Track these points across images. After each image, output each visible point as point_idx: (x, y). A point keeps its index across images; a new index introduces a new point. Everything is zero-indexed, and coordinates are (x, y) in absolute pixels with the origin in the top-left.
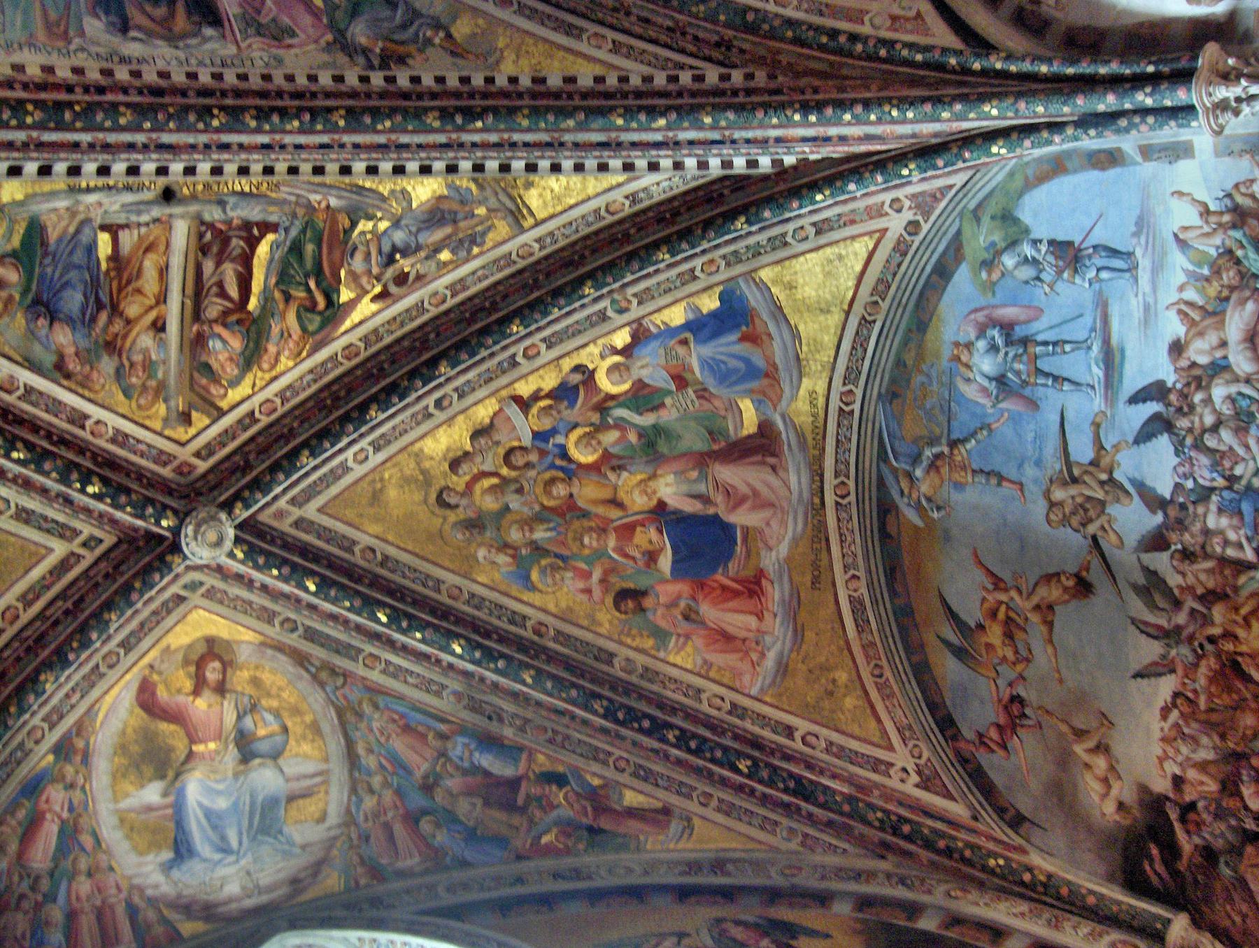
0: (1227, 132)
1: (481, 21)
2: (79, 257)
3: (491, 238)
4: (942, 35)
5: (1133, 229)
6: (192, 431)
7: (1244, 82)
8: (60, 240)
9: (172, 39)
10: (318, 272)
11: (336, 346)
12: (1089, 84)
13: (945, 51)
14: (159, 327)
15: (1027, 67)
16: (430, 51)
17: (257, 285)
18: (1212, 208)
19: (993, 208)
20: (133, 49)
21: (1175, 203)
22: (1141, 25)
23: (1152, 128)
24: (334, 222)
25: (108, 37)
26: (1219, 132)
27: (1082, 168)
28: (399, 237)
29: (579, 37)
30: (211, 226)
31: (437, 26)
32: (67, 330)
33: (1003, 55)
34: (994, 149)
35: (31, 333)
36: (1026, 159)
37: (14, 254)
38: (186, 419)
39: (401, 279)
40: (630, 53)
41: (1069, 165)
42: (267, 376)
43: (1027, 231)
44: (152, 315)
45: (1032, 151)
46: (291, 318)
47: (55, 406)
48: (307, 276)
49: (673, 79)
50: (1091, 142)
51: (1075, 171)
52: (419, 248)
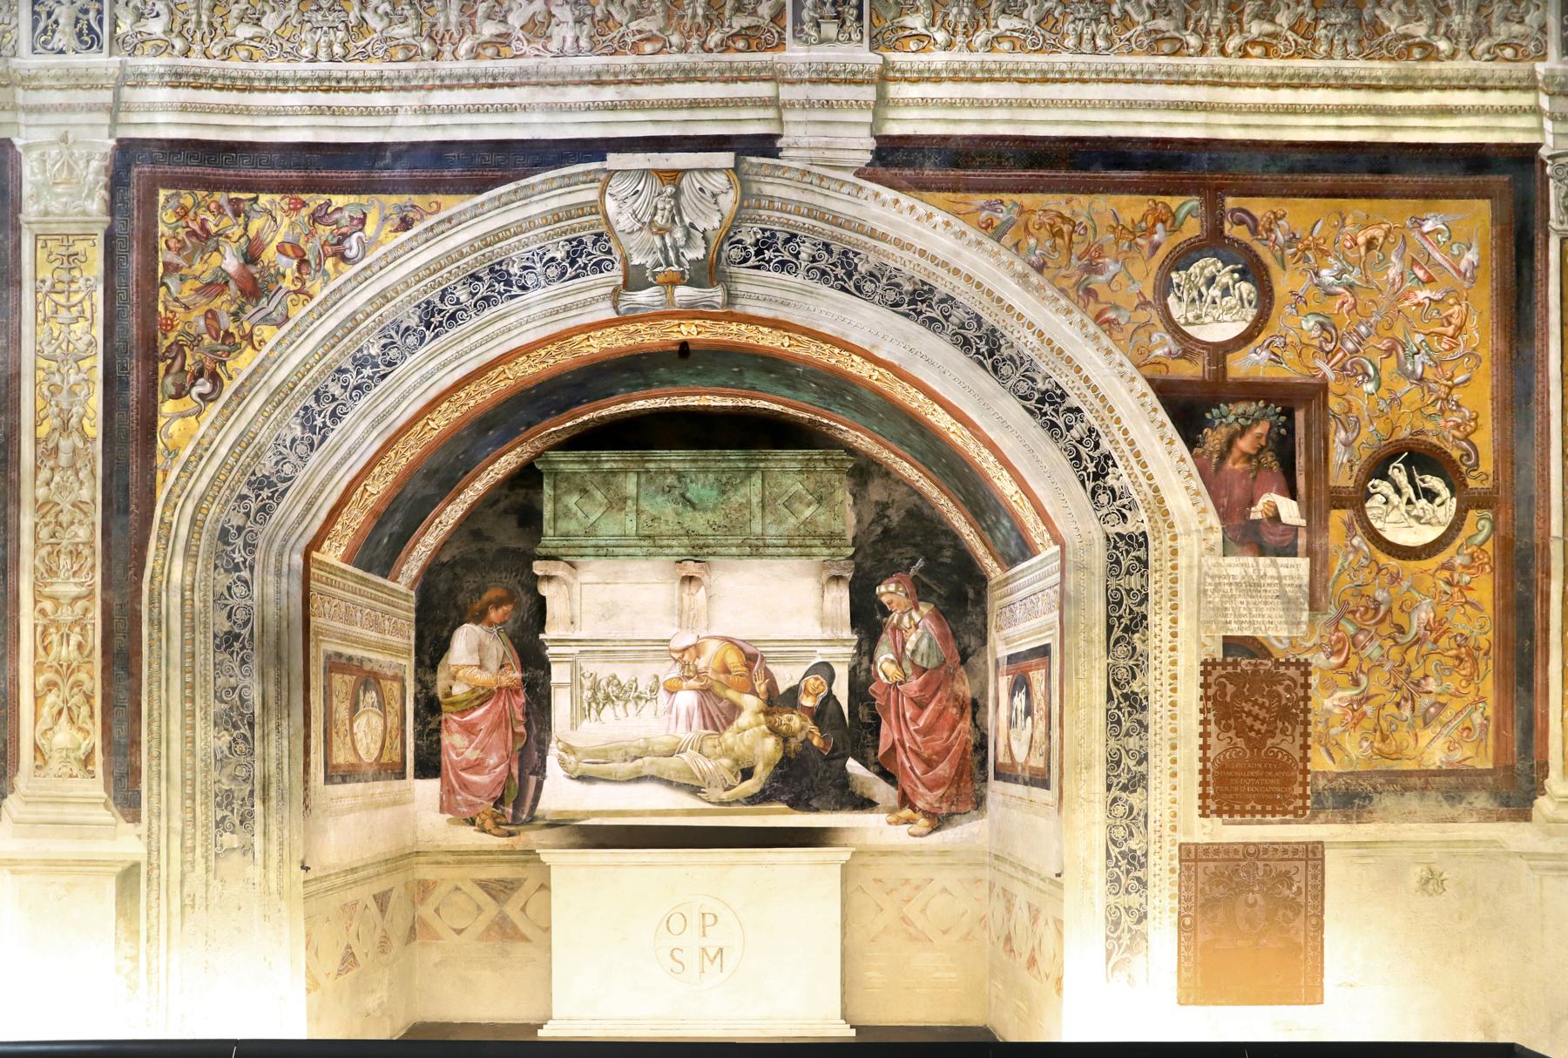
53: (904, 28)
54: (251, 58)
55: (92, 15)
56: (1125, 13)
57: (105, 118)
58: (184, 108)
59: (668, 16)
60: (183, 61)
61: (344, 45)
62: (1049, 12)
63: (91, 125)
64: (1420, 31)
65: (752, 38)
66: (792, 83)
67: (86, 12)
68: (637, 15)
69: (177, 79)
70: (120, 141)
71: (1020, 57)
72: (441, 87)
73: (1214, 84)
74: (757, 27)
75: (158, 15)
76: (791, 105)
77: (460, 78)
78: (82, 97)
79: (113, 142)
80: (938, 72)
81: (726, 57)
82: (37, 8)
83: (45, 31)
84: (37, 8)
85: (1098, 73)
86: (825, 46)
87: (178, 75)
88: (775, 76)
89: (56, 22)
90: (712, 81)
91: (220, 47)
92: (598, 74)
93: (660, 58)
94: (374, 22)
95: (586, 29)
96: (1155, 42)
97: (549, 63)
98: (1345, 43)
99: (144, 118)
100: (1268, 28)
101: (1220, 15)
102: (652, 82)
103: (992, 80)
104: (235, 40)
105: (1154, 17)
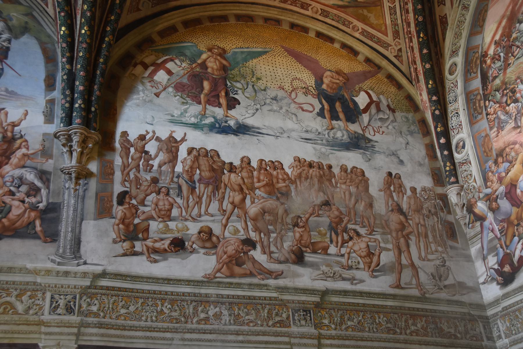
0: (55, 140)
4: (126, 19)
5: (10, 89)
7: (79, 150)
12: (90, 81)
13: (119, 16)
15: (104, 52)
18: (16, 128)
19: (32, 24)
21: (21, 111)
22: (116, 110)
23: (62, 105)
26: (56, 136)
27: (47, 71)
33: (112, 42)
34: (63, 28)
36: (56, 45)
41: (50, 65)
43: (16, 37)
45: (59, 48)
50: (60, 76)
51: (46, 67)
53: (323, 323)
54: (125, 319)
55: (72, 303)
56: (380, 322)
57: (74, 338)
58: (102, 335)
59: (257, 316)
60: (103, 320)
61: (156, 317)
62: (360, 321)
63: (69, 340)
64: (452, 331)
65: (281, 323)
66: (294, 338)
67: (70, 302)
68: (247, 314)
69: (100, 326)
70: (79, 346)
71: (355, 333)
72: (188, 332)
73: (405, 343)
74: (283, 321)
75: (95, 305)
76: (294, 344)
77: (194, 330)
78: (66, 330)
79: (76, 346)
80: (334, 336)
81: (275, 329)
82: (53, 300)
83: (55, 307)
84: (53, 300)
85: (376, 338)
86: (302, 327)
87: (101, 324)
88: (289, 335)
89: (59, 305)
90: (271, 336)
91: (115, 316)
92: (237, 331)
93: (255, 328)
94: (165, 310)
95: (232, 317)
96: (389, 331)
97: (221, 327)
98: (435, 333)
99: (85, 338)
100: (416, 328)
101: (403, 324)
102: (253, 335)
103: (348, 339)
104: (120, 313)
105: (387, 323)
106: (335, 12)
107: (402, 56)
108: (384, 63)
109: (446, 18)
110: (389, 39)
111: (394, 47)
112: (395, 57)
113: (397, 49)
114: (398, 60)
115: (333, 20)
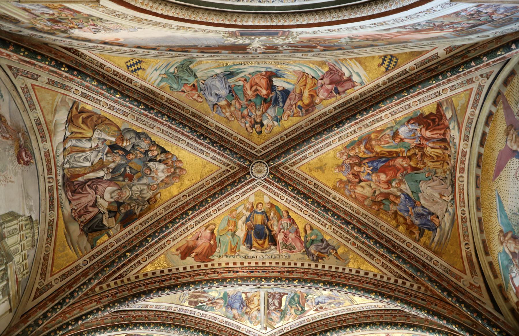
1: (346, 249)
2: (237, 297)
3: (345, 304)
6: (267, 331)
8: (232, 295)
9: (262, 250)
10: (299, 303)
11: (305, 318)
14: (259, 310)
16: (330, 256)
17: (283, 304)
20: (252, 254)
24: (302, 295)
25: (246, 251)
28: (320, 300)
29: (373, 259)
30: (270, 293)
31: (334, 249)
32: (236, 311)
35: (227, 311)
37: (221, 298)
38: (266, 328)
39: (321, 308)
40: (386, 267)
42: (287, 322)
44: (257, 308)
46: (293, 311)
47: (233, 325)
48: (296, 303)
49: (396, 281)
52: (325, 303)
106: (463, 131)
107: (486, 73)
108: (495, 88)
109: (447, 49)
110: (474, 86)
111: (480, 81)
112: (488, 78)
113: (481, 79)
114: (490, 76)
115: (469, 132)
